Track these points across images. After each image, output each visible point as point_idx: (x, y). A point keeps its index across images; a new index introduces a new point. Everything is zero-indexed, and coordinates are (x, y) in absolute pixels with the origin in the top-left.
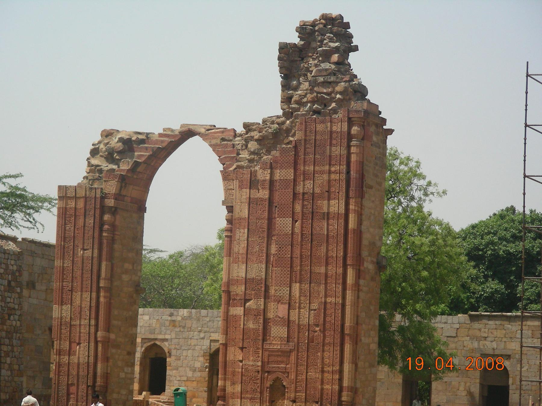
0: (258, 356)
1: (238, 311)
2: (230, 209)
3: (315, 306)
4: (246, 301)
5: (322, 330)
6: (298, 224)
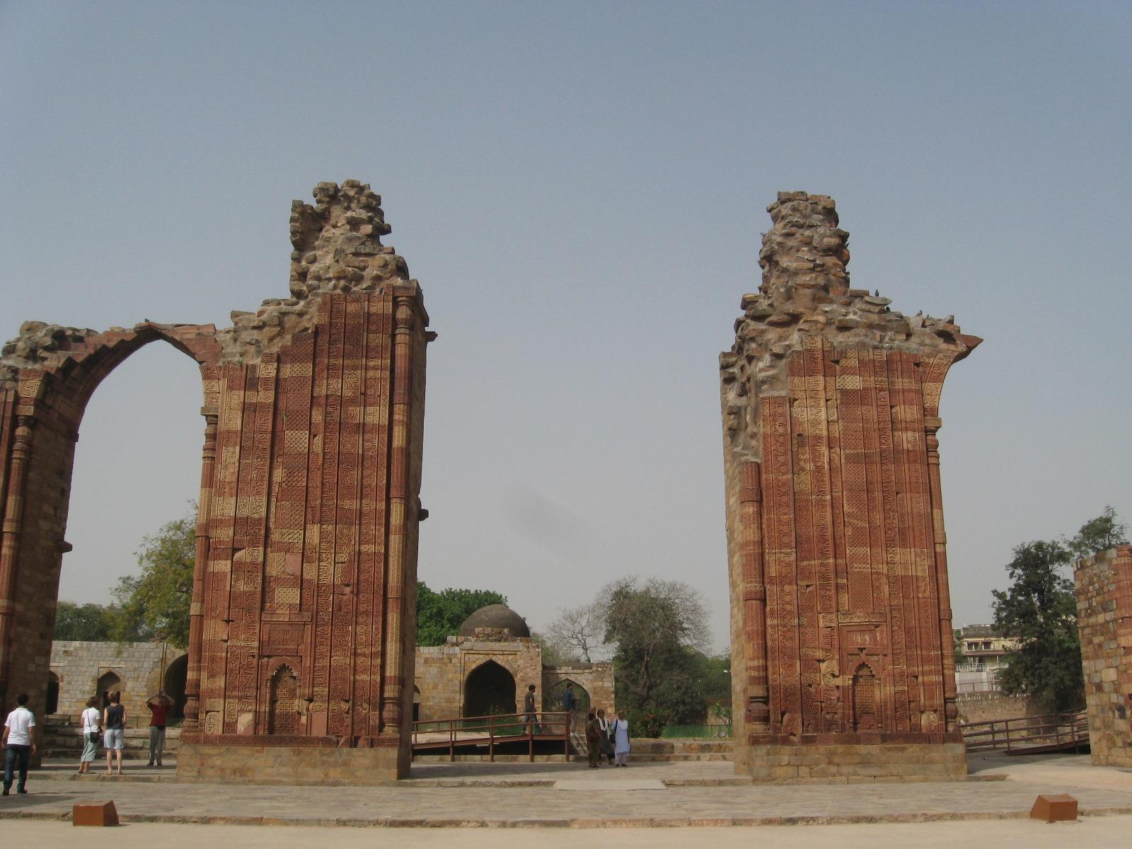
1: (223, 566)
2: (212, 419)
3: (343, 557)
4: (235, 550)
5: (355, 592)
6: (318, 441)
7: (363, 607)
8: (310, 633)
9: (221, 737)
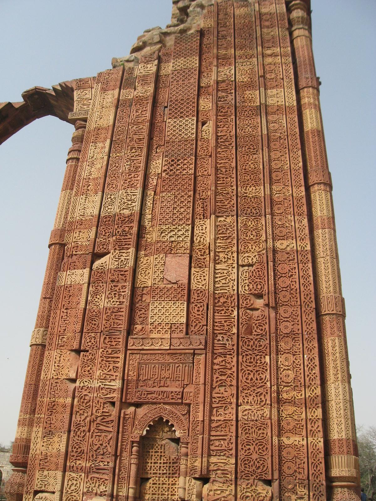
3: (251, 257)
4: (96, 256)
5: (272, 304)
6: (209, 127)
7: (286, 327)
8: (202, 366)
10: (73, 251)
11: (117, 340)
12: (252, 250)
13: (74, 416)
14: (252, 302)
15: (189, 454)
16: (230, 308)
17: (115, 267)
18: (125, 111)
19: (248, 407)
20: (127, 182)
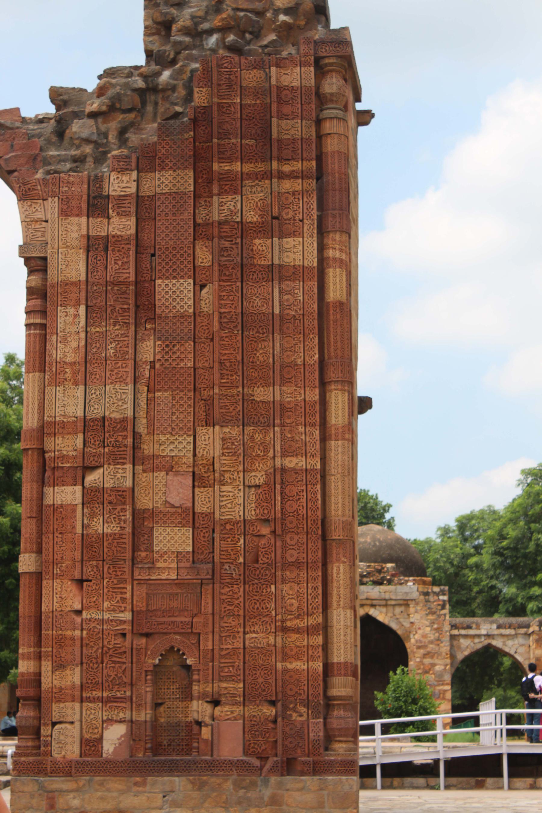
0: (124, 600)
1: (68, 495)
3: (258, 478)
4: (88, 469)
7: (292, 556)
9: (77, 762)
10: (58, 463)
11: (121, 569)
12: (259, 469)
13: (84, 648)
14: (258, 528)
15: (201, 680)
16: (236, 536)
17: (111, 486)
18: (99, 258)
19: (254, 635)
20: (114, 373)
